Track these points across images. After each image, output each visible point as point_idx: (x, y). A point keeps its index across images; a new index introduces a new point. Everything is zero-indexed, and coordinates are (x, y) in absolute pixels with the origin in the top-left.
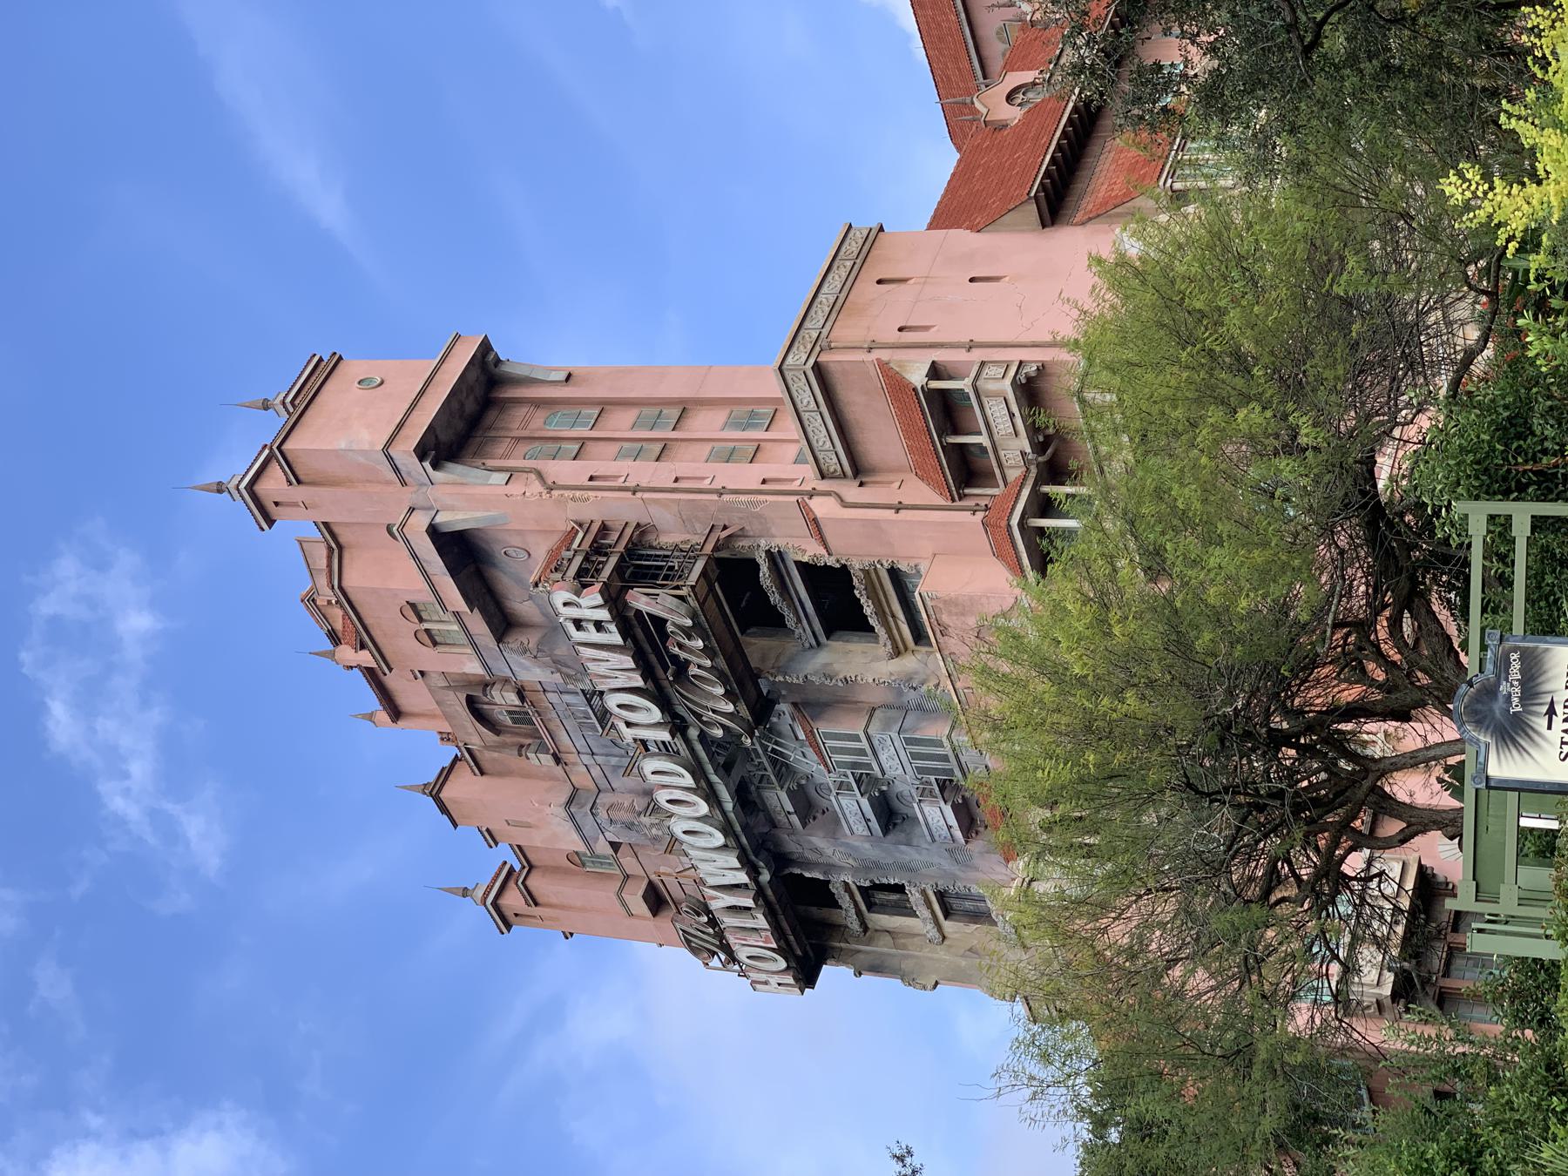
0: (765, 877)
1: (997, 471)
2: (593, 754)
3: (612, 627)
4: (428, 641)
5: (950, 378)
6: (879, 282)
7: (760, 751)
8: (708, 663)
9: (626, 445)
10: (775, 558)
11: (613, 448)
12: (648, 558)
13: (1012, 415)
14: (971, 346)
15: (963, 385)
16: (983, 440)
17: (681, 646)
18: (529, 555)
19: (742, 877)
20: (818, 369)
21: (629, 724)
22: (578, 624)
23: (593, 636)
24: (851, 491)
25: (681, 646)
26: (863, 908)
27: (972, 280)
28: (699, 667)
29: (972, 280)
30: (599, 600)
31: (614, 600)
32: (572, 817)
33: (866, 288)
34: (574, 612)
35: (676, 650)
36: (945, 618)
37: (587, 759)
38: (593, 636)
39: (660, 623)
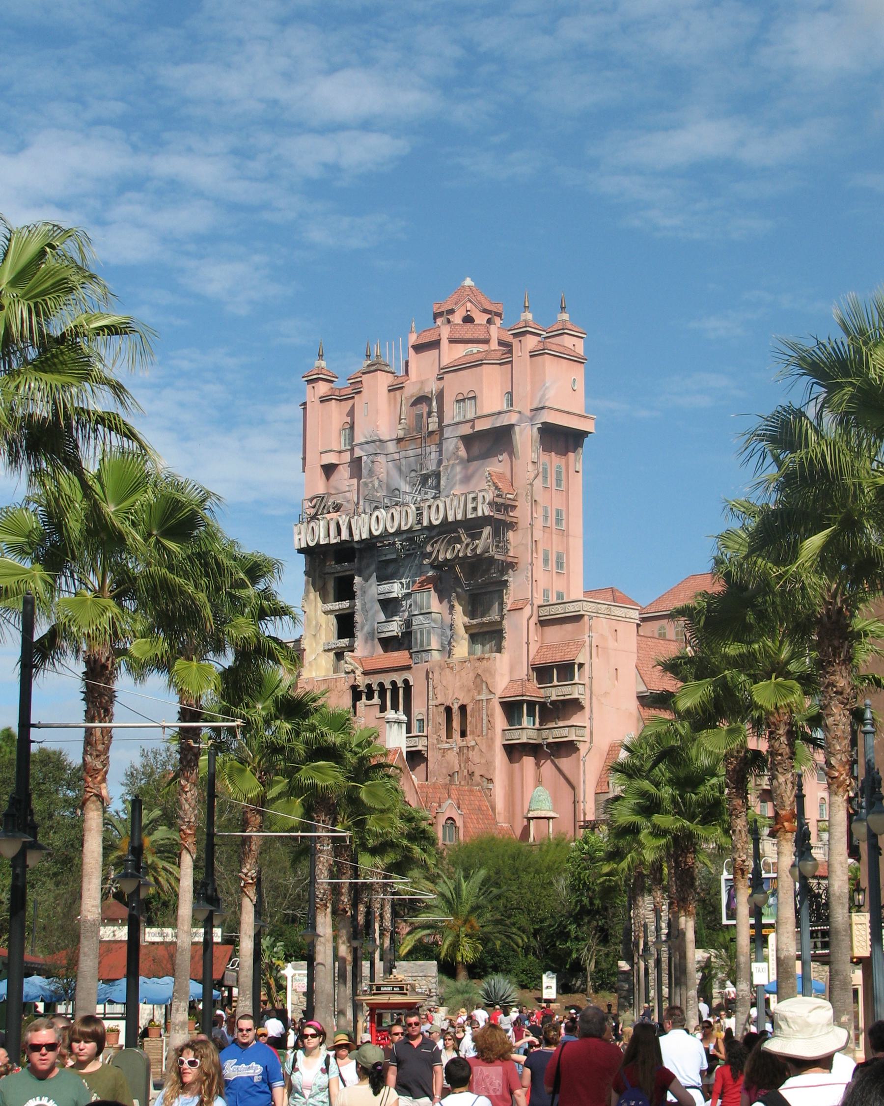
0: (356, 546)
3: (473, 516)
5: (579, 669)
14: (591, 678)
15: (576, 680)
16: (555, 683)
20: (582, 616)
21: (429, 507)
22: (474, 499)
23: (470, 506)
24: (534, 619)
26: (336, 575)
28: (459, 551)
30: (486, 514)
31: (485, 520)
32: (373, 442)
34: (480, 499)
38: (470, 506)
39: (478, 536)
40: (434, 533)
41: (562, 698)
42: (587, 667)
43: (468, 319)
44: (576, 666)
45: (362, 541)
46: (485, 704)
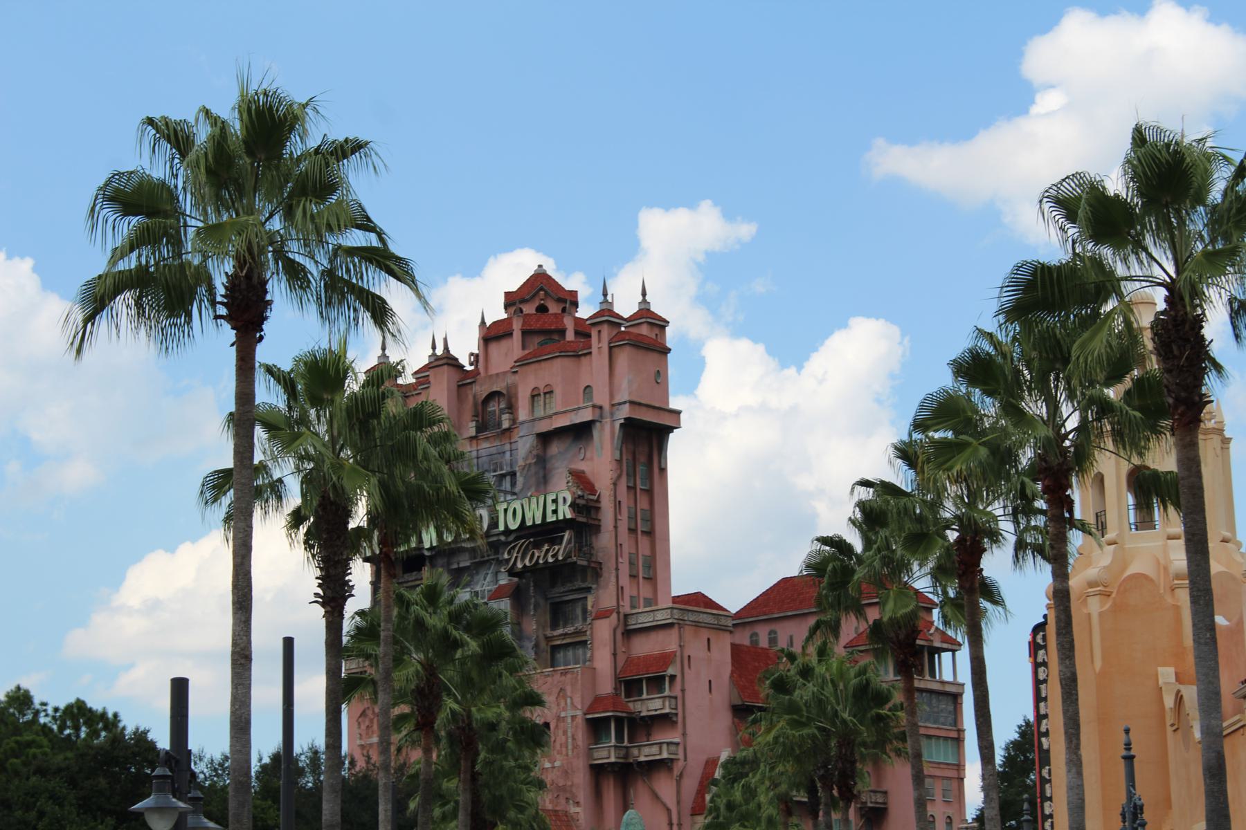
0: (426, 553)
1: (632, 699)
2: (478, 458)
3: (554, 519)
4: (535, 393)
6: (709, 640)
7: (491, 557)
8: (541, 562)
9: (633, 510)
10: (588, 590)
11: (632, 505)
12: (586, 537)
13: (656, 710)
14: (683, 691)
15: (667, 693)
16: (645, 696)
17: (547, 551)
18: (583, 460)
19: (427, 545)
21: (506, 510)
22: (555, 501)
23: (551, 507)
25: (547, 551)
27: (710, 681)
28: (539, 557)
29: (710, 681)
30: (569, 516)
31: (566, 524)
33: (705, 634)
34: (560, 501)
35: (546, 547)
36: (569, 676)
37: (474, 454)
40: (511, 538)
41: (654, 713)
42: (679, 679)
43: (542, 309)
44: (667, 679)
45: (432, 548)
46: (569, 720)
